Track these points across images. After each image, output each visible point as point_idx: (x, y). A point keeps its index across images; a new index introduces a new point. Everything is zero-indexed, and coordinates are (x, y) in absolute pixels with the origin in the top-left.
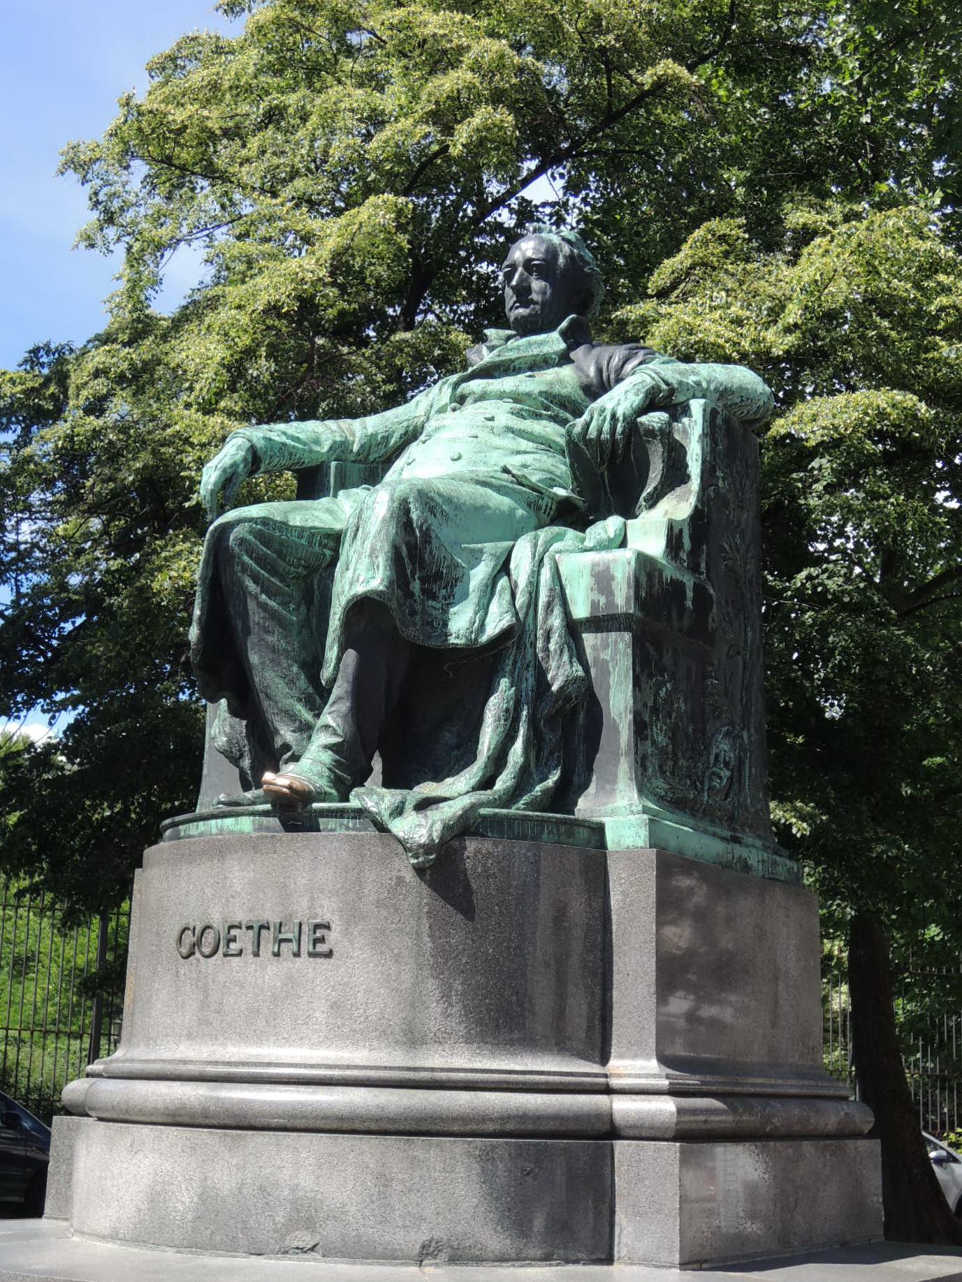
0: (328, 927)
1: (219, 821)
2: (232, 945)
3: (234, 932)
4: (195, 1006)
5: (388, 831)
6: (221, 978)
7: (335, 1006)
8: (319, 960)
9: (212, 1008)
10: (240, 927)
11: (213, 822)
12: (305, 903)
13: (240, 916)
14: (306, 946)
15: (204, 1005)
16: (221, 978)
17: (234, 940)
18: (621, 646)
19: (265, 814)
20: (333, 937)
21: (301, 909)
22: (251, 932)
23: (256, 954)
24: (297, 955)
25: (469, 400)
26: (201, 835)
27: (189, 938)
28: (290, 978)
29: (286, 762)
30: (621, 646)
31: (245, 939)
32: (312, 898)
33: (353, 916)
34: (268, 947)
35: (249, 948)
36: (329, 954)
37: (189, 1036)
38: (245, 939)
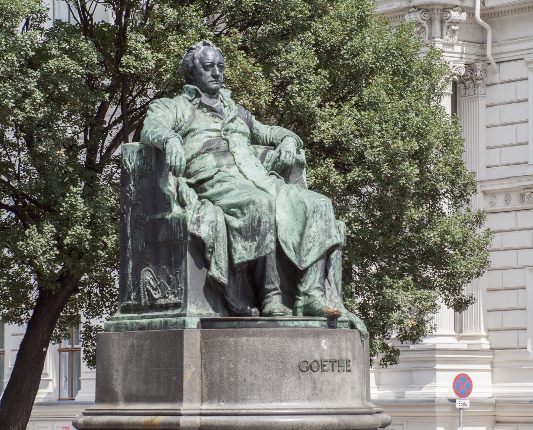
0: (350, 361)
1: (305, 322)
2: (325, 368)
3: (325, 363)
4: (310, 389)
5: (357, 329)
6: (321, 379)
7: (352, 388)
8: (349, 373)
9: (319, 389)
10: (327, 361)
11: (302, 322)
12: (345, 354)
13: (327, 358)
14: (345, 369)
15: (314, 389)
16: (321, 379)
17: (325, 366)
18: (339, 256)
19: (325, 321)
20: (351, 364)
21: (344, 354)
22: (331, 364)
23: (333, 371)
24: (344, 371)
25: (229, 132)
26: (296, 327)
27: (305, 365)
28: (342, 379)
29: (275, 295)
30: (339, 256)
31: (328, 366)
32: (346, 352)
33: (354, 359)
34: (336, 369)
35: (331, 369)
36: (350, 371)
37: (309, 399)
38: (328, 366)
